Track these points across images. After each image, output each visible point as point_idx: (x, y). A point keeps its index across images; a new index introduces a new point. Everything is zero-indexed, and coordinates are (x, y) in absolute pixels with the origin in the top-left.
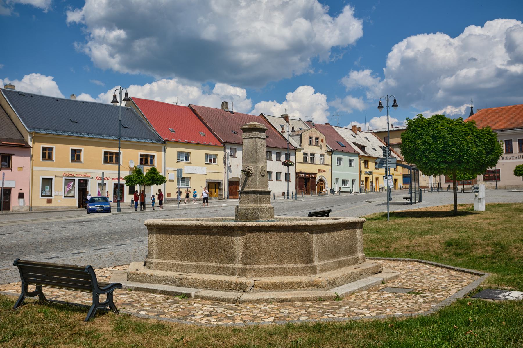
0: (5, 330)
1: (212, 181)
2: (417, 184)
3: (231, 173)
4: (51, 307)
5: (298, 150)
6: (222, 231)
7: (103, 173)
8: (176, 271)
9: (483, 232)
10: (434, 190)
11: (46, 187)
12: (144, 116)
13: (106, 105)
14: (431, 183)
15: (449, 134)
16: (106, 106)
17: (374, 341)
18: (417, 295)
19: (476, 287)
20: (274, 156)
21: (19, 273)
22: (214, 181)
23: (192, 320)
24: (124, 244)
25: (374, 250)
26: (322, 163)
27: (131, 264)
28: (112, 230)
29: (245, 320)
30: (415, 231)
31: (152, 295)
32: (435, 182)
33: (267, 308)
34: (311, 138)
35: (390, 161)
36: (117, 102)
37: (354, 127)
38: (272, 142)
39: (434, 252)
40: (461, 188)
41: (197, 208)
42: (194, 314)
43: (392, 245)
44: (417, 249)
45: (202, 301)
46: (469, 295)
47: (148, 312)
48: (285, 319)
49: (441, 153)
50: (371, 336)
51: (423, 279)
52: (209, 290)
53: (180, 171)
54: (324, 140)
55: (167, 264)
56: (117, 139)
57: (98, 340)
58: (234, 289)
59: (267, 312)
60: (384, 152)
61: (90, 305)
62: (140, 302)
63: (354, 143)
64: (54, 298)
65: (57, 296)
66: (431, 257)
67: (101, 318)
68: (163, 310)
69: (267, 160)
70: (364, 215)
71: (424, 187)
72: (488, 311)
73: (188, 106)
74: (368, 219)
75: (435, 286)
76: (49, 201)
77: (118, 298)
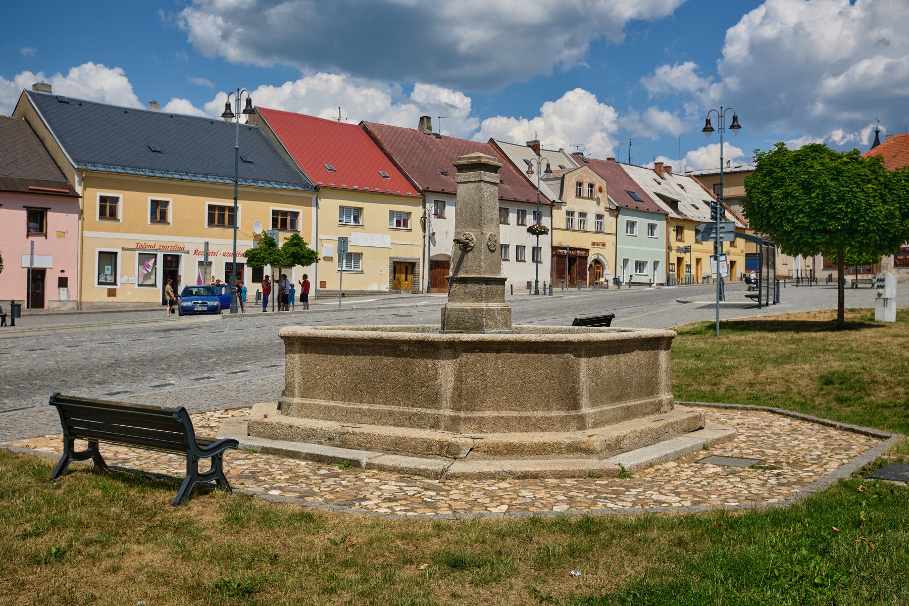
0: (37, 515)
1: (401, 260)
2: (771, 271)
3: (434, 246)
4: (114, 478)
5: (556, 207)
6: (417, 349)
7: (207, 244)
8: (335, 420)
9: (890, 361)
10: (802, 282)
11: (106, 267)
12: (280, 142)
13: (212, 122)
14: (797, 270)
15: (832, 180)
16: (212, 123)
17: (687, 552)
18: (767, 471)
19: (874, 459)
20: (513, 217)
21: (59, 418)
22: (405, 261)
23: (362, 508)
24: (242, 371)
25: (690, 388)
26: (599, 231)
27: (255, 406)
28: (222, 346)
29: (455, 509)
30: (766, 356)
31: (292, 462)
32: (804, 269)
33: (496, 488)
34: (580, 184)
35: (724, 228)
36: (232, 115)
37: (658, 165)
38: (511, 192)
39: (799, 394)
40: (852, 280)
41: (374, 309)
42: (365, 496)
43: (724, 380)
44: (768, 388)
45: (380, 474)
46: (862, 474)
47: (285, 491)
48: (527, 509)
49: (817, 216)
50: (680, 543)
51: (777, 443)
52: (392, 454)
53: (343, 241)
54: (604, 189)
55: (319, 406)
56: (232, 182)
57: (196, 538)
58: (438, 453)
59: (496, 496)
60: (712, 212)
61: (182, 476)
62: (270, 474)
63: (659, 195)
64: (121, 463)
65: (125, 461)
66: (794, 403)
67: (202, 500)
68: (311, 489)
69: (501, 223)
70: (674, 326)
71: (785, 278)
72: (896, 502)
73: (359, 124)
74: (681, 334)
75: (800, 456)
76: (112, 293)
77: (232, 465)
